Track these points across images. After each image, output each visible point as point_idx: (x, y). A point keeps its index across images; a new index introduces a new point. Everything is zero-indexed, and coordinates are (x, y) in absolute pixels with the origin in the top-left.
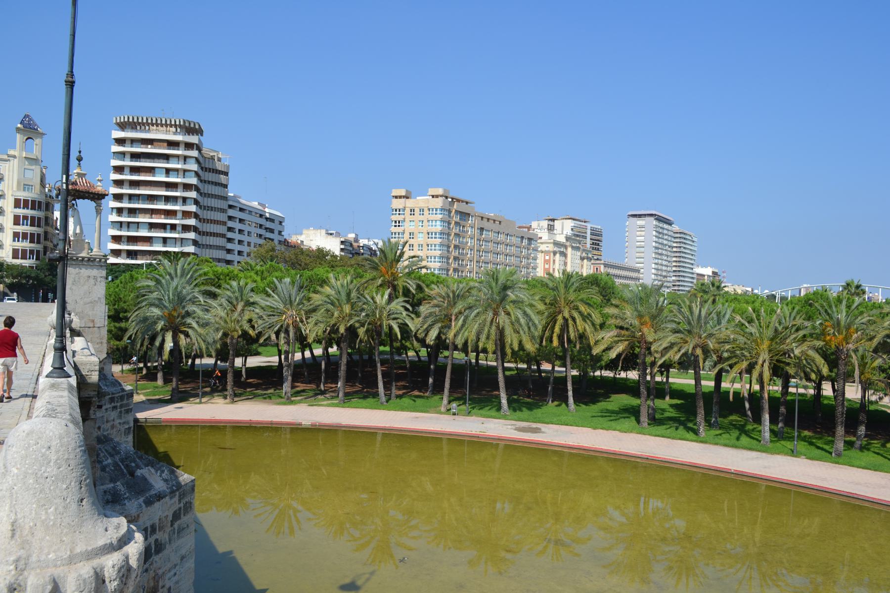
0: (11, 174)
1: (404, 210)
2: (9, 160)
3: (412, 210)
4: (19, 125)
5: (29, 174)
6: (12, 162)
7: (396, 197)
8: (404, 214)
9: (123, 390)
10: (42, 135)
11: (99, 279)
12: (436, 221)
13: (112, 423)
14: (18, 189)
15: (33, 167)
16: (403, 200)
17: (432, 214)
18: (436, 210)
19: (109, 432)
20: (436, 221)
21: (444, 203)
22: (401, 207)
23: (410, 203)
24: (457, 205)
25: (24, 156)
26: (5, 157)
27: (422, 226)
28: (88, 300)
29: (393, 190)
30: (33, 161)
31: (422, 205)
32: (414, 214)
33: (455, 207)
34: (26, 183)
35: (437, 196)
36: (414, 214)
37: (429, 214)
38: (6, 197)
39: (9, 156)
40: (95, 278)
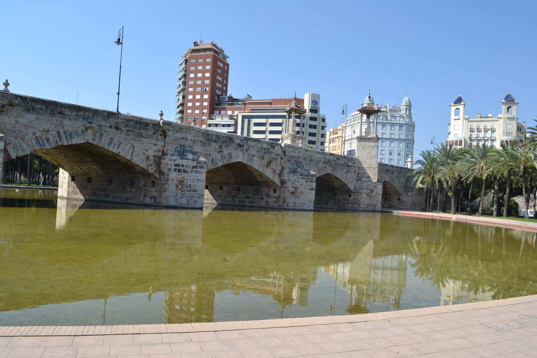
0: (499, 127)
2: (498, 120)
4: (503, 101)
5: (509, 127)
6: (500, 121)
9: (309, 173)
10: (517, 103)
11: (374, 147)
13: (301, 183)
14: (503, 135)
15: (512, 122)
19: (299, 186)
25: (506, 117)
26: (496, 119)
28: (369, 156)
30: (513, 119)
34: (508, 132)
38: (497, 140)
39: (498, 118)
40: (372, 147)
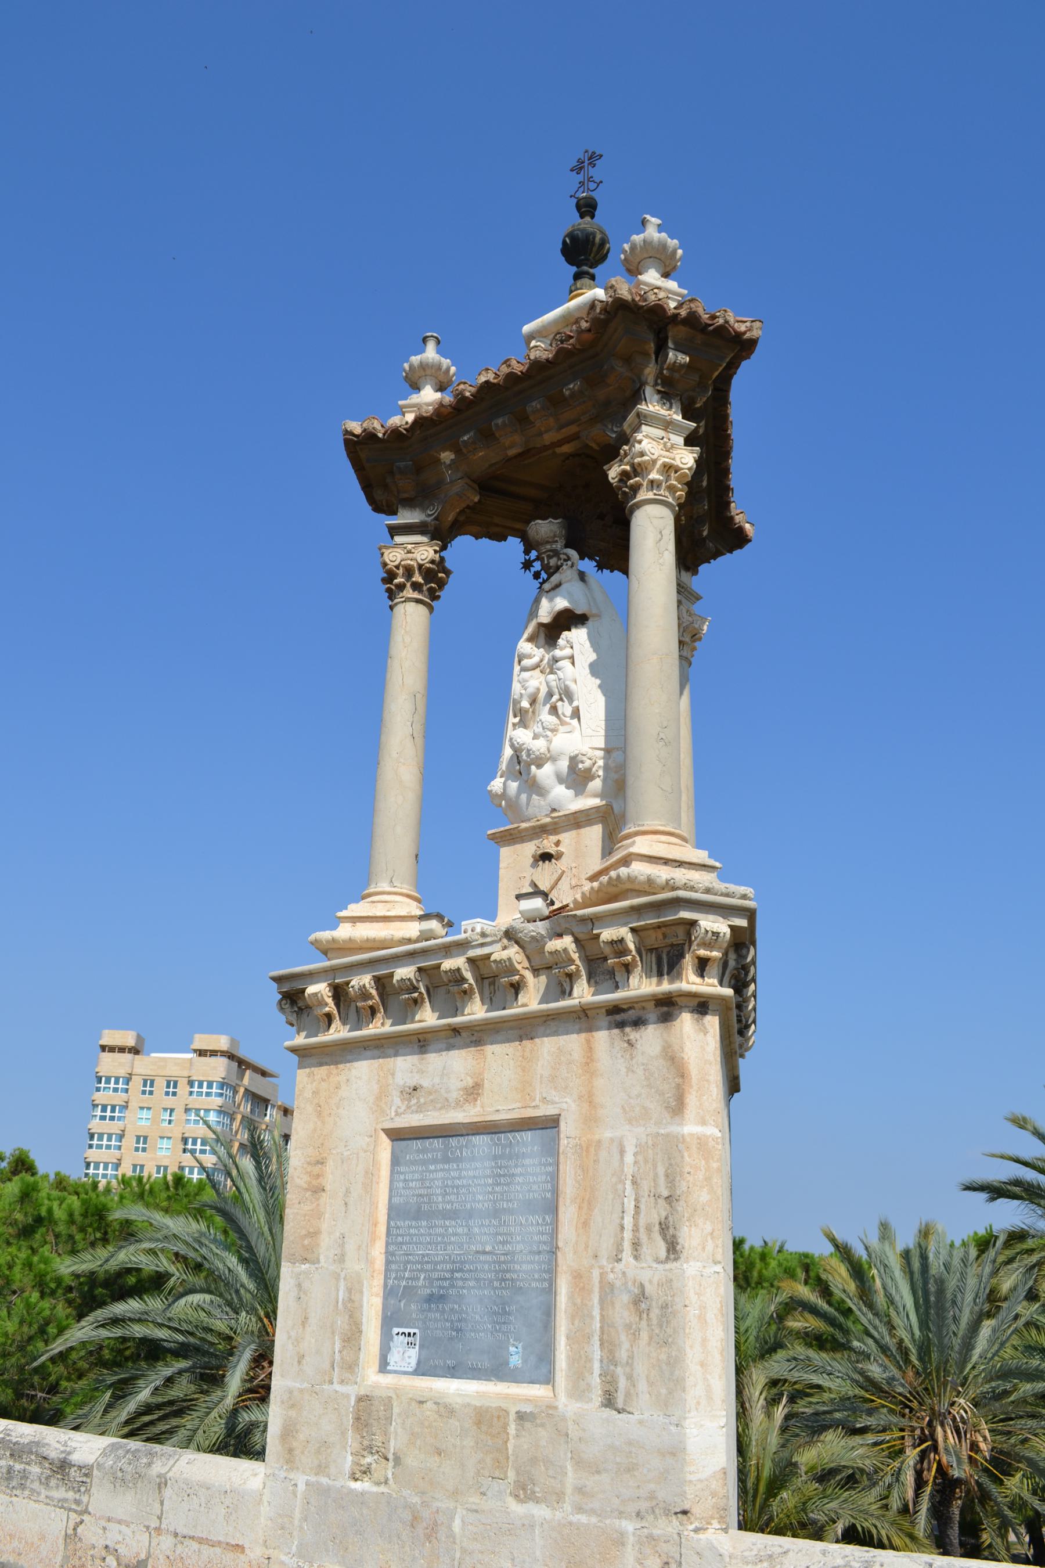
1: (128, 1081)
3: (149, 1082)
7: (112, 1049)
8: (127, 1091)
12: (207, 1111)
16: (128, 1056)
17: (200, 1094)
18: (210, 1085)
20: (207, 1111)
21: (228, 1071)
22: (122, 1072)
23: (142, 1065)
24: (251, 1079)
27: (170, 1122)
29: (106, 1032)
31: (173, 1071)
32: (151, 1093)
33: (246, 1081)
35: (213, 1053)
36: (151, 1093)
37: (191, 1093)
